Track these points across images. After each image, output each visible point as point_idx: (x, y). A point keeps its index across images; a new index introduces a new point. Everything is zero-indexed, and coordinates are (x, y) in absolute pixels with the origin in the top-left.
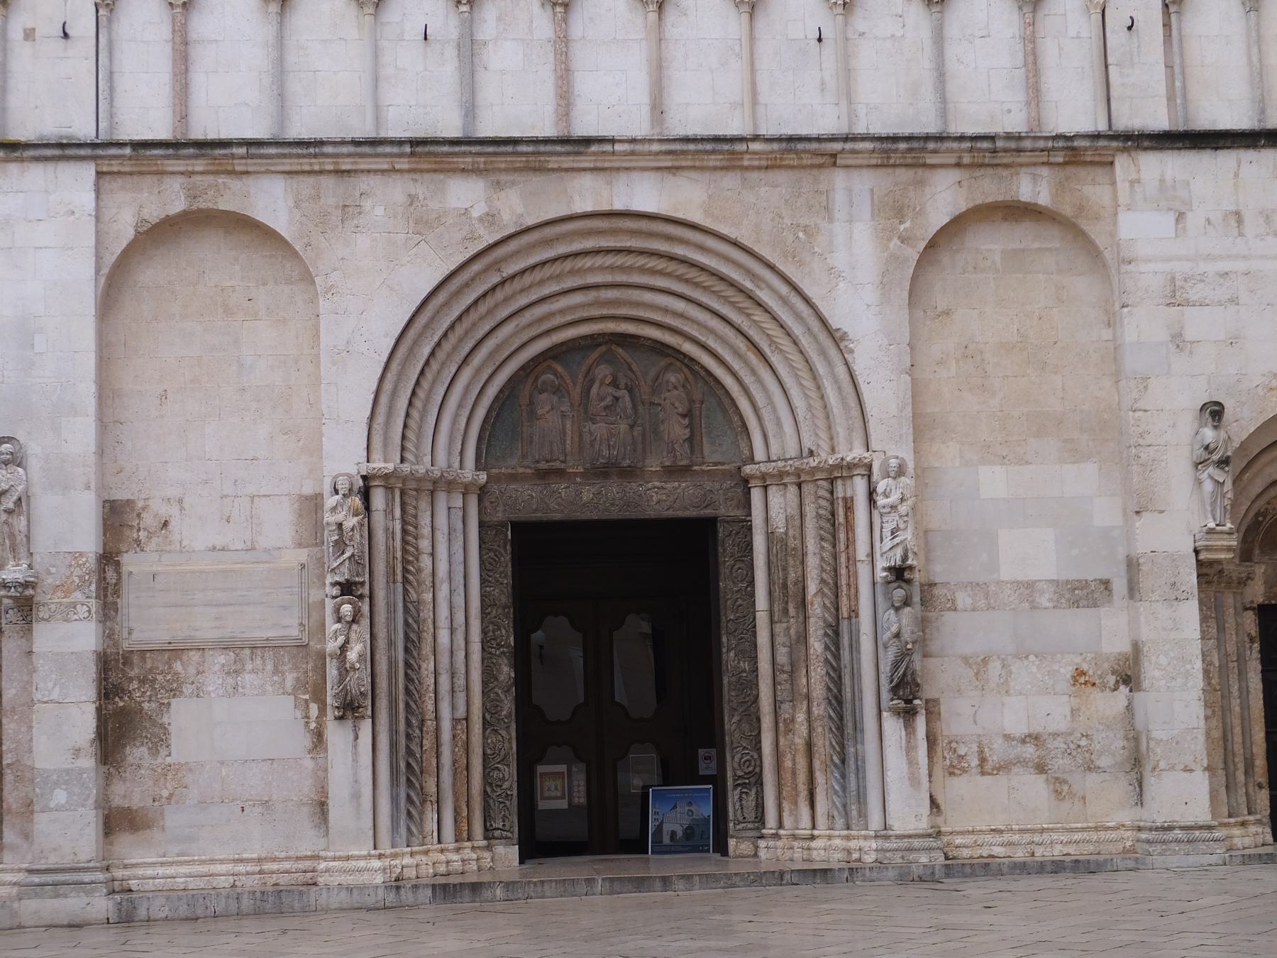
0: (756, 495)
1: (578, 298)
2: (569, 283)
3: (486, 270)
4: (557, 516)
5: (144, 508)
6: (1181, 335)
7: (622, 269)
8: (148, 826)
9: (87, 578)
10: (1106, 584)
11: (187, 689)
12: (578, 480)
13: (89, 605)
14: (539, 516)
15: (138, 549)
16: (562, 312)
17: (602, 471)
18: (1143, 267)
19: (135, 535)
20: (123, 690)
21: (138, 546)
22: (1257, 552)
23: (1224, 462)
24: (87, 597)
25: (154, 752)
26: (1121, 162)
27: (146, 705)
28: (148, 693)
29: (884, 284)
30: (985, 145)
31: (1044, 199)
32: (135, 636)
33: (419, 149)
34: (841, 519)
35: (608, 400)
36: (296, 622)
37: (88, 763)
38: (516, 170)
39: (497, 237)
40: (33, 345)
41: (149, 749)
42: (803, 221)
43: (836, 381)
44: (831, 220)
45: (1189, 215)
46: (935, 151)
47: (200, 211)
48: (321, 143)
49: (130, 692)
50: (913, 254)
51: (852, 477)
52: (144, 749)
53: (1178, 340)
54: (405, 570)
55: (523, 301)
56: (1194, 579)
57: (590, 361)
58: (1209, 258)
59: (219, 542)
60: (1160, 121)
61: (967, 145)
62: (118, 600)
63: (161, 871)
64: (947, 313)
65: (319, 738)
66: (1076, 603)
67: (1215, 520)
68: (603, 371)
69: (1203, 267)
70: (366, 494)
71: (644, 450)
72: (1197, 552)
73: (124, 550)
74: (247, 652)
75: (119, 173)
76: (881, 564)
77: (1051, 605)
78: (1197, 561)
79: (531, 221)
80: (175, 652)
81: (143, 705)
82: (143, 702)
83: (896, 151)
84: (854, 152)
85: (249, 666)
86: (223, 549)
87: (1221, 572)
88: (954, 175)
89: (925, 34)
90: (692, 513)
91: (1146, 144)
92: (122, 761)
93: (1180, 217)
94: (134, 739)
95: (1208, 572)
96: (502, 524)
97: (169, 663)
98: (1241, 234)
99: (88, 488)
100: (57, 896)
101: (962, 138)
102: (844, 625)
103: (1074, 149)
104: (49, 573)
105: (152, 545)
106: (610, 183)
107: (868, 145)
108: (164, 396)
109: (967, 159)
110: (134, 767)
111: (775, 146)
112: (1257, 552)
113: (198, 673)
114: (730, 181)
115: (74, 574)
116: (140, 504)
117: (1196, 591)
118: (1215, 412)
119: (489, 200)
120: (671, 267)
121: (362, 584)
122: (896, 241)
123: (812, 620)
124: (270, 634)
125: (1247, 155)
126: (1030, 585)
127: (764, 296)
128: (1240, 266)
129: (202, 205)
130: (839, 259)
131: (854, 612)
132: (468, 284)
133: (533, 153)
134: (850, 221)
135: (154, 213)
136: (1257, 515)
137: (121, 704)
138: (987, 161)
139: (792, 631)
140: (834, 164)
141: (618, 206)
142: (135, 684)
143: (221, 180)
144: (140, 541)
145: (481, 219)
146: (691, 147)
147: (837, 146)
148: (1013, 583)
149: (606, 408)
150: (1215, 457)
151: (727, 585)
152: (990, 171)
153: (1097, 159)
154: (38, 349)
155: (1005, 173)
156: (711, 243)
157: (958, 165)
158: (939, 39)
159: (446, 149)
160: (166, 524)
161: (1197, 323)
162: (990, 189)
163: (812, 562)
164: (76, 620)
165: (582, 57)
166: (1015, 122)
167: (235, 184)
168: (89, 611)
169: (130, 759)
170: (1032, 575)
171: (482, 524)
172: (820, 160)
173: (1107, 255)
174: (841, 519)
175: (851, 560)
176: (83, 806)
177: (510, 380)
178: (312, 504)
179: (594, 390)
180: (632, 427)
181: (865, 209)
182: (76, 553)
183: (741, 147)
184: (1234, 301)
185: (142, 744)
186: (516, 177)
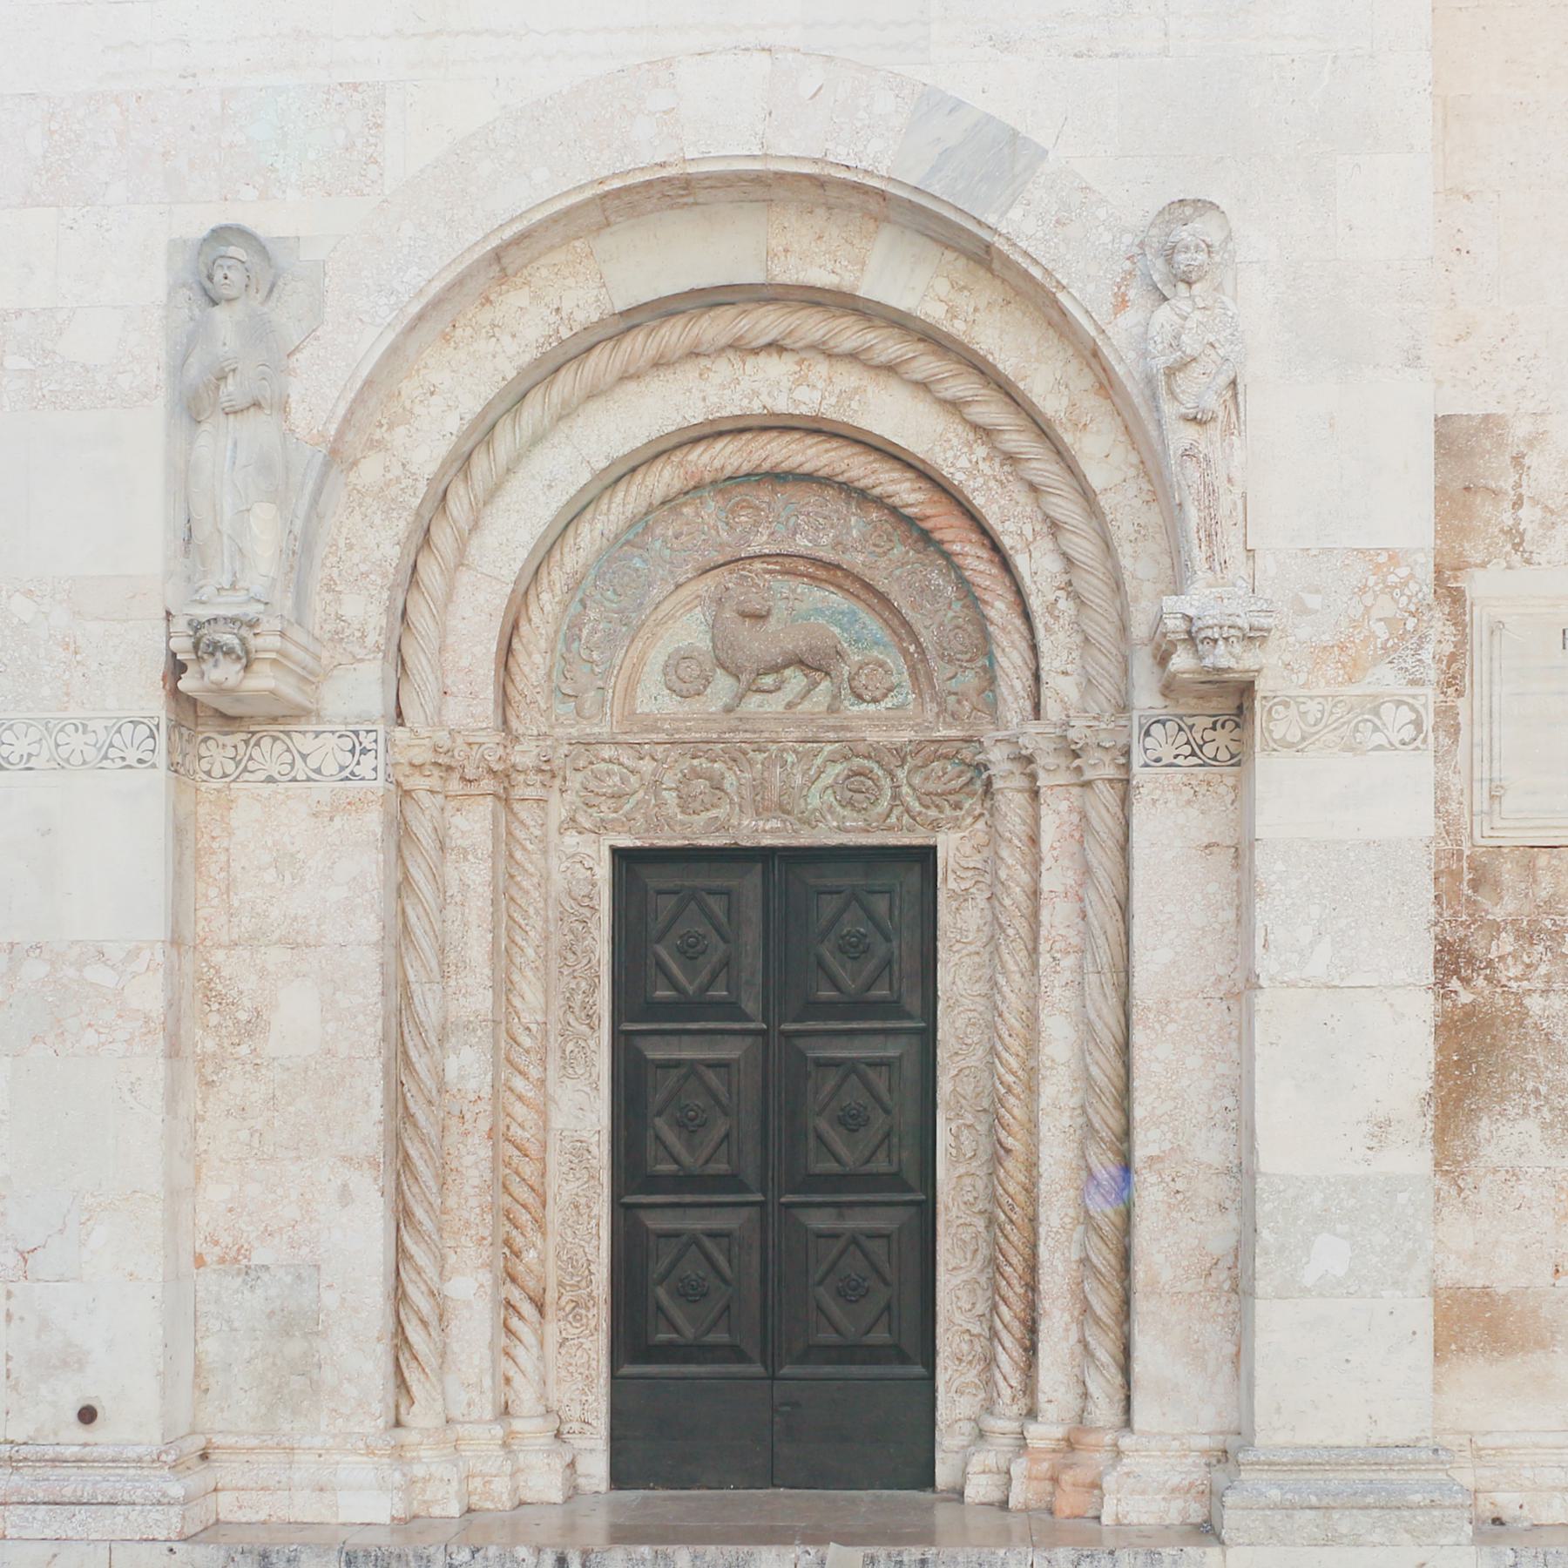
5: (1531, 444)
9: (1410, 625)
13: (1417, 705)
15: (1516, 558)
19: (1507, 519)
20: (1471, 960)
21: (1516, 547)
24: (1413, 682)
27: (1534, 1003)
28: (1543, 970)
41: (1545, 1126)
49: (1490, 963)
52: (1530, 1126)
62: (1461, 704)
73: (1477, 558)
81: (1527, 1001)
82: (1529, 992)
92: (1466, 1159)
94: (1502, 1098)
104: (1303, 610)
110: (1502, 1175)
115: (1375, 613)
137: (1465, 997)
142: (1507, 943)
144: (1522, 535)
164: (1379, 748)
168: (1418, 724)
169: (1490, 1154)
176: (1395, 1283)
182: (1378, 553)
185: (1525, 1113)
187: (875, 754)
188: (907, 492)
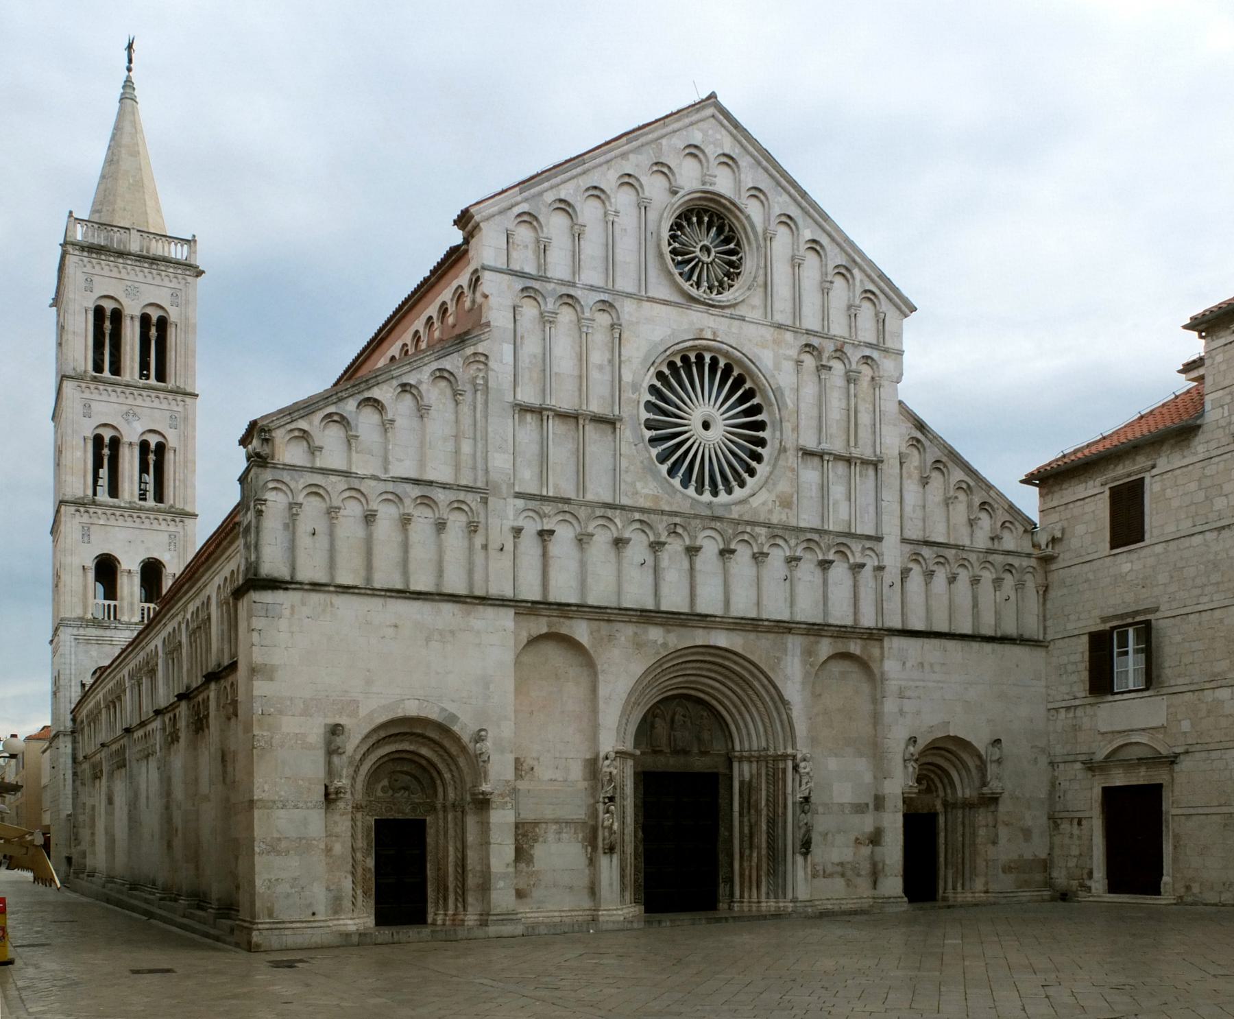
0: (736, 765)
1: (680, 679)
4: (660, 770)
7: (699, 668)
8: (526, 897)
11: (541, 839)
14: (653, 770)
16: (671, 685)
17: (677, 752)
18: (893, 682)
25: (528, 865)
26: (886, 640)
27: (524, 846)
29: (803, 683)
30: (843, 629)
31: (858, 652)
32: (521, 816)
33: (644, 614)
37: (511, 870)
38: (677, 625)
39: (667, 653)
40: (489, 689)
42: (777, 655)
43: (781, 721)
44: (786, 655)
46: (826, 630)
47: (553, 633)
48: (606, 608)
50: (813, 671)
51: (785, 760)
52: (524, 864)
53: (901, 712)
58: (913, 680)
59: (554, 777)
61: (838, 629)
63: (532, 915)
64: (820, 695)
65: (592, 862)
68: (679, 709)
69: (911, 683)
74: (564, 824)
75: (522, 614)
80: (536, 824)
83: (813, 629)
84: (799, 628)
85: (565, 831)
86: (555, 781)
89: (821, 581)
91: (896, 633)
97: (533, 828)
99: (512, 752)
100: (504, 925)
101: (837, 626)
103: (871, 633)
105: (527, 778)
106: (708, 633)
108: (532, 713)
109: (835, 635)
111: (772, 624)
113: (545, 833)
114: (752, 636)
116: (522, 760)
119: (664, 638)
120: (720, 669)
122: (808, 666)
124: (575, 817)
125: (926, 640)
127: (756, 683)
128: (921, 684)
129: (554, 630)
130: (789, 671)
133: (686, 619)
134: (793, 656)
135: (535, 633)
140: (789, 633)
143: (562, 620)
145: (661, 645)
146: (743, 621)
151: (722, 802)
152: (841, 639)
154: (491, 690)
155: (846, 640)
156: (741, 661)
157: (831, 636)
158: (825, 583)
159: (653, 614)
160: (532, 769)
161: (908, 706)
162: (841, 647)
165: (700, 578)
166: (849, 621)
167: (567, 622)
172: (785, 631)
173: (878, 676)
178: (593, 766)
181: (798, 652)
184: (919, 698)
186: (675, 628)
187: (417, 804)
188: (424, 763)
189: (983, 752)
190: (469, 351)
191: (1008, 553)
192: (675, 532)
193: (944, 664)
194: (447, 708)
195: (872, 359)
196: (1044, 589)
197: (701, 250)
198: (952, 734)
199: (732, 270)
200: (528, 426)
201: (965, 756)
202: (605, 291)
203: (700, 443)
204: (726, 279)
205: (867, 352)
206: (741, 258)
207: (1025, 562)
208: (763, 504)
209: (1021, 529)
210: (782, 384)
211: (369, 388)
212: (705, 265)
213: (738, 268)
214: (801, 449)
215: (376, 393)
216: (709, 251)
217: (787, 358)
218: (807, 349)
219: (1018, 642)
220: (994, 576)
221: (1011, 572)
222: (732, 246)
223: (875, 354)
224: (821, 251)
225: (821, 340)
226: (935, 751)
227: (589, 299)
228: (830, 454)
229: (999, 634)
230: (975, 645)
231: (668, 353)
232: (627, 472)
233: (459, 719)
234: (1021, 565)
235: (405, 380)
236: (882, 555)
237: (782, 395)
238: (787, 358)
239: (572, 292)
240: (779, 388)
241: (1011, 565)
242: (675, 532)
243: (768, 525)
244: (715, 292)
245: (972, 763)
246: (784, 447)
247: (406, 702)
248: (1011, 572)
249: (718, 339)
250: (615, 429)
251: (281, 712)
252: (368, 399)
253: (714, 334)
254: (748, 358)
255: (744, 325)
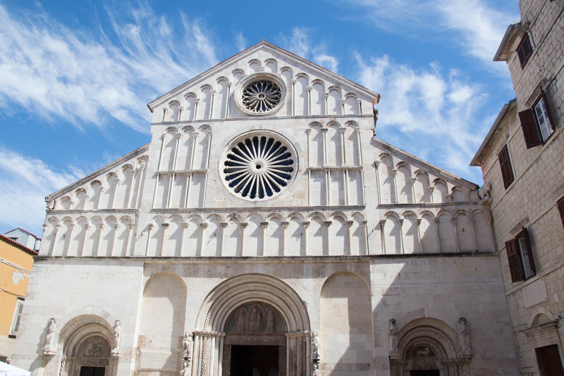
0: (288, 340)
2: (245, 289)
3: (225, 286)
4: (242, 344)
5: (147, 337)
6: (385, 303)
10: (369, 364)
12: (247, 335)
22: (410, 356)
23: (395, 334)
32: (141, 367)
34: (304, 347)
35: (255, 317)
36: (176, 366)
45: (387, 274)
48: (189, 258)
54: (202, 356)
55: (235, 293)
56: (389, 364)
57: (252, 307)
60: (380, 252)
66: (361, 369)
67: (393, 349)
70: (194, 337)
71: (263, 329)
72: (390, 357)
74: (165, 372)
76: (312, 358)
77: (355, 370)
78: (390, 359)
79: (234, 275)
86: (162, 348)
87: (397, 362)
88: (332, 265)
90: (273, 344)
91: (376, 258)
93: (385, 274)
95: (393, 362)
96: (229, 345)
98: (400, 279)
102: (304, 373)
107: (311, 259)
112: (410, 356)
116: (146, 337)
117: (389, 367)
118: (393, 322)
119: (226, 270)
121: (190, 358)
123: (297, 372)
124: (170, 369)
126: (350, 365)
128: (400, 286)
131: (306, 370)
132: (221, 289)
136: (410, 347)
138: (339, 262)
139: (293, 374)
141: (254, 272)
145: (223, 275)
147: (304, 259)
148: (345, 364)
149: (255, 319)
150: (394, 332)
153: (365, 261)
155: (344, 264)
157: (333, 263)
160: (151, 341)
163: (298, 357)
170: (350, 362)
171: (224, 345)
172: (299, 262)
174: (304, 347)
175: (306, 357)
177: (233, 311)
179: (252, 315)
180: (260, 323)
183: (282, 259)
184: (398, 294)
189: (454, 327)
190: (140, 156)
191: (459, 204)
192: (234, 218)
193: (416, 273)
194: (105, 310)
195: (355, 122)
196: (490, 221)
197: (260, 96)
198: (426, 316)
199: (275, 100)
200: (164, 181)
201: (446, 330)
202: (204, 121)
203: (254, 175)
204: (271, 104)
205: (351, 119)
206: (281, 95)
207: (473, 208)
208: (286, 198)
209: (467, 190)
210: (298, 141)
211: (96, 177)
212: (261, 102)
213: (279, 99)
214: (310, 169)
215: (98, 178)
216: (264, 96)
217: (300, 129)
218: (314, 124)
219: (473, 255)
220: (452, 217)
221: (465, 214)
222: (275, 91)
223: (355, 119)
224: (322, 83)
225: (322, 119)
226: (423, 328)
227: (196, 126)
228: (328, 168)
229: (458, 251)
230: (440, 260)
231: (236, 139)
232: (209, 193)
233: (110, 315)
234: (470, 209)
235: (111, 171)
236: (366, 215)
237: (299, 146)
238: (300, 129)
239: (190, 124)
240: (297, 143)
241: (464, 210)
242: (234, 218)
243: (289, 209)
244: (266, 110)
245: (451, 335)
246: (300, 169)
247: (87, 307)
248: (465, 214)
249: (262, 129)
250: (205, 175)
251: (33, 313)
252: (96, 181)
253: (260, 127)
254: (279, 134)
255: (278, 121)
